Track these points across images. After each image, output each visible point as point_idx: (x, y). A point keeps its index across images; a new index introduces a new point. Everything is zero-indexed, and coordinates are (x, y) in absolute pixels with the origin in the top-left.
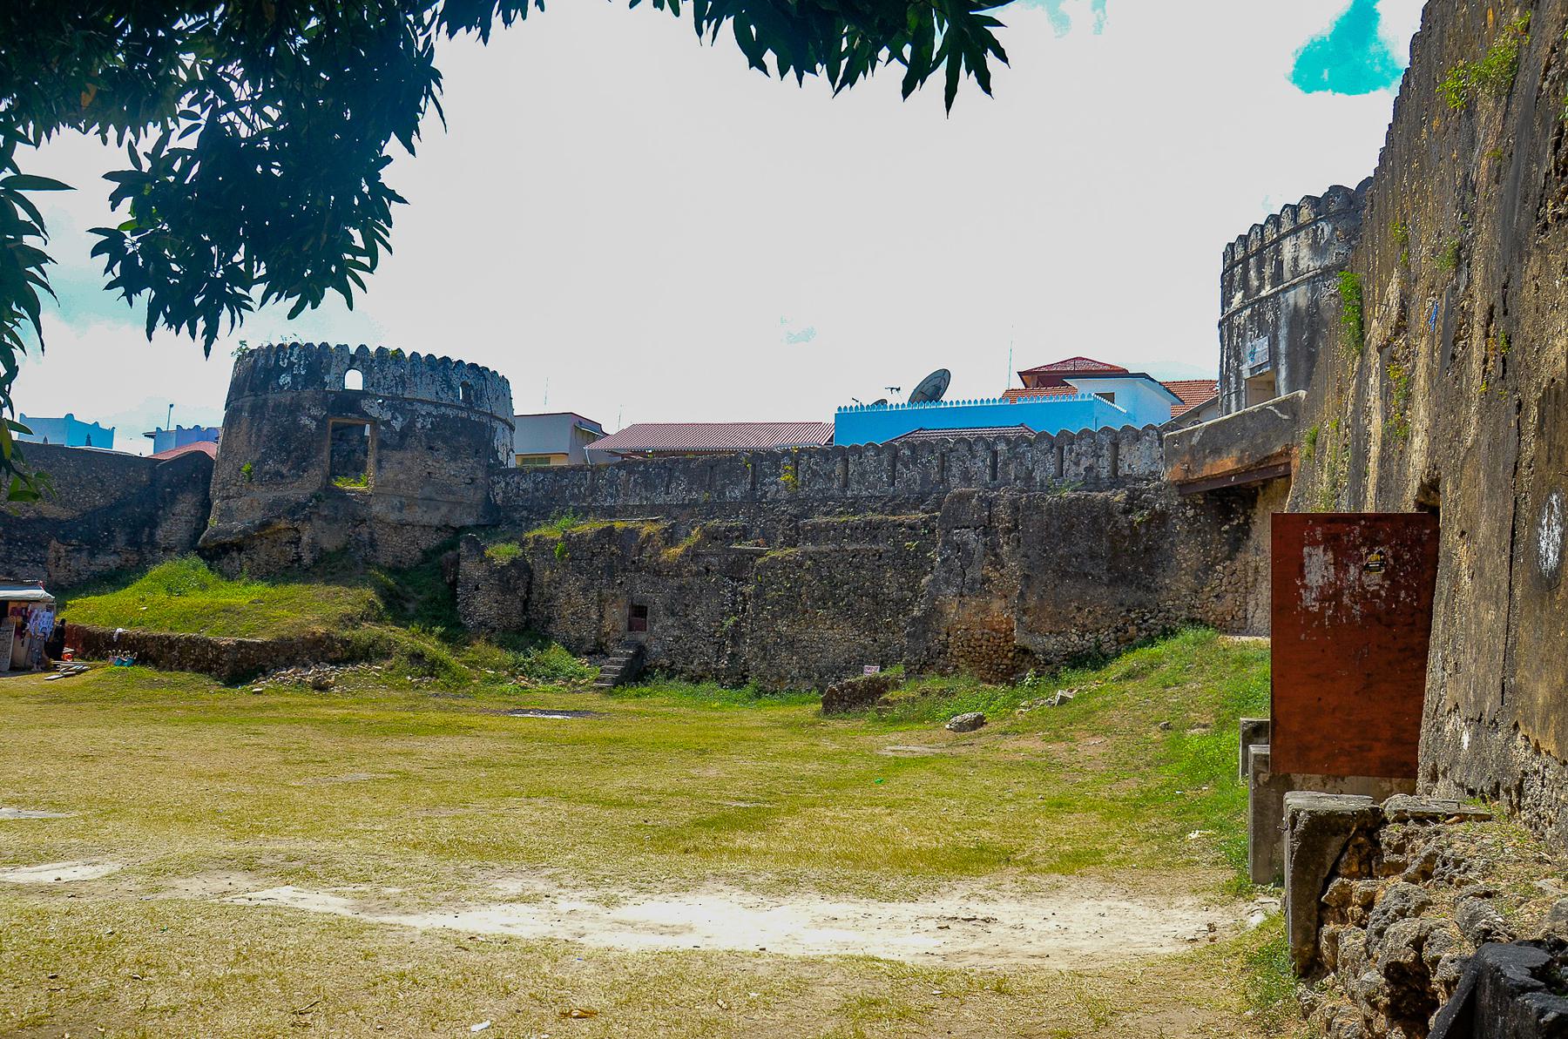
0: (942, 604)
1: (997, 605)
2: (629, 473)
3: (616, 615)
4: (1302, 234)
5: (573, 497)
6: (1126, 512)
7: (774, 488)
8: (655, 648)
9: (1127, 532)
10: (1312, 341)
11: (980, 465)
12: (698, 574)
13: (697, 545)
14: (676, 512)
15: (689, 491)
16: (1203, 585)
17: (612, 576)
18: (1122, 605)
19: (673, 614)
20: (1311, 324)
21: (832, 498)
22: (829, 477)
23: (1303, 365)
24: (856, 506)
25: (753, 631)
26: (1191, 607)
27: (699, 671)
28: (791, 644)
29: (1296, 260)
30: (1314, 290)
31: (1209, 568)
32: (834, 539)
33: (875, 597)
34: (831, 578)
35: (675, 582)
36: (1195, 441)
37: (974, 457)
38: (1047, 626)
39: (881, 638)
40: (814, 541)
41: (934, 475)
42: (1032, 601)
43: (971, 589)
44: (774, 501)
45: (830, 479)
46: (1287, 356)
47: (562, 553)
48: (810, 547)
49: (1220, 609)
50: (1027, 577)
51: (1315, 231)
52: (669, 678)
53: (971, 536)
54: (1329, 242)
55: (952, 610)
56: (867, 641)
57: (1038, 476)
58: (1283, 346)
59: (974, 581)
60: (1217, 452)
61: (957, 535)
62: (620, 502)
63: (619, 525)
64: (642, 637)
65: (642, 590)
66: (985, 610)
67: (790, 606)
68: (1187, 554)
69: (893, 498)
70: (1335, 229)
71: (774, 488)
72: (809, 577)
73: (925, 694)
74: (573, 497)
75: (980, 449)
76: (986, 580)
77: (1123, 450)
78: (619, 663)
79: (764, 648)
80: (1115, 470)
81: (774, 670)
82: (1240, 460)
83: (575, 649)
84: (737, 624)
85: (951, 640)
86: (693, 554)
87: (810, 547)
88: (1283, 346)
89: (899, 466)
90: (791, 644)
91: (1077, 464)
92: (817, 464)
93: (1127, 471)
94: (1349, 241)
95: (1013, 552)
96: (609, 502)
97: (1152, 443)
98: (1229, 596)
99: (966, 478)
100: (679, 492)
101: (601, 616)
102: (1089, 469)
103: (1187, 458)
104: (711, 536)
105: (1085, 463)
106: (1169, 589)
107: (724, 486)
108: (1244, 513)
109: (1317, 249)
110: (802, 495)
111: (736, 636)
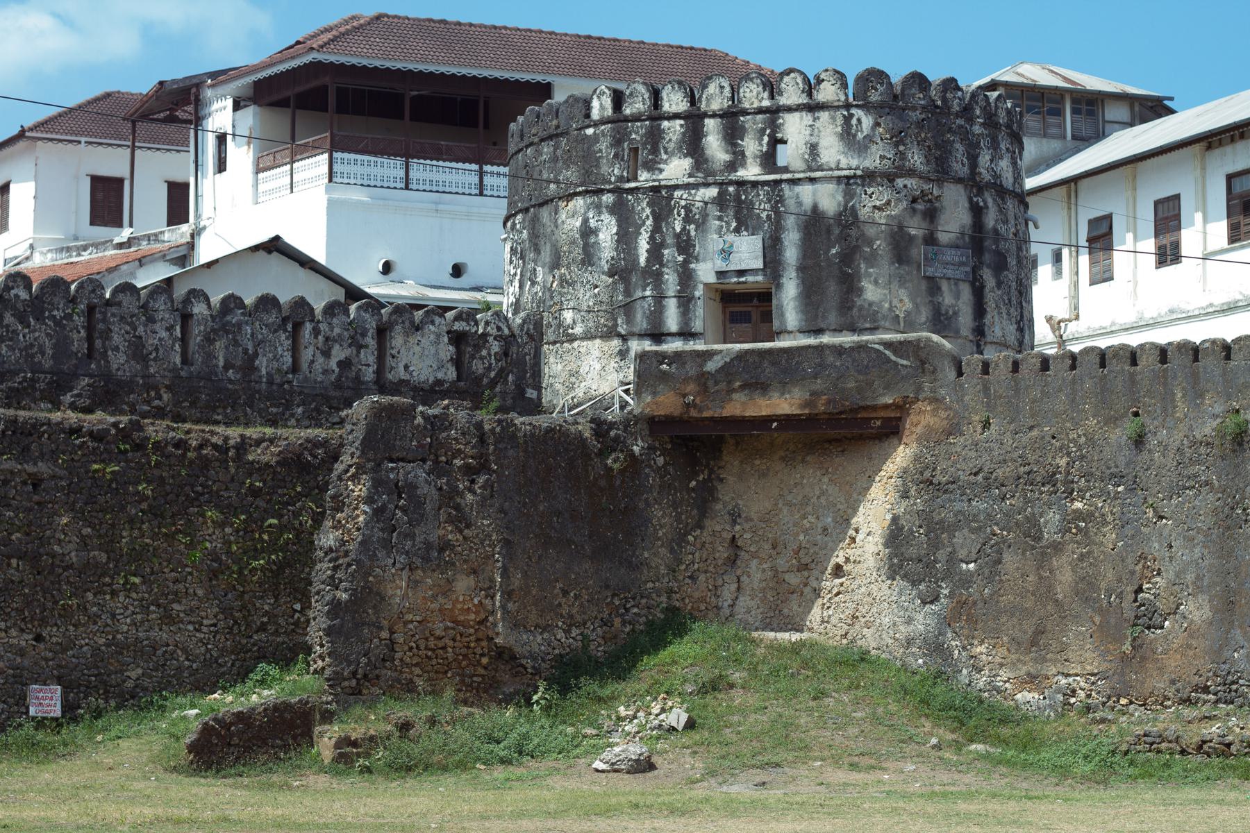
1: (463, 584)
4: (824, 116)
6: (602, 454)
9: (603, 483)
10: (848, 257)
11: (161, 334)
16: (680, 562)
18: (607, 587)
20: (844, 237)
23: (833, 288)
26: (670, 592)
29: (813, 148)
30: (849, 195)
31: (681, 539)
33: (34, 559)
36: (711, 366)
38: (533, 618)
39: (54, 634)
41: (78, 340)
42: (517, 580)
43: (426, 559)
46: (802, 269)
49: (696, 595)
50: (507, 543)
51: (848, 119)
53: (419, 473)
54: (869, 139)
55: (398, 589)
57: (262, 363)
58: (791, 254)
59: (429, 546)
60: (758, 386)
61: (397, 472)
66: (446, 590)
68: (661, 518)
70: (877, 124)
73: (405, 727)
75: (160, 304)
76: (445, 546)
77: (397, 340)
80: (380, 372)
82: (807, 404)
85: (400, 638)
88: (791, 254)
91: (327, 354)
93: (402, 375)
94: (897, 145)
95: (483, 504)
97: (438, 336)
98: (702, 577)
99: (137, 350)
102: (345, 364)
103: (691, 387)
105: (339, 353)
106: (650, 567)
108: (707, 466)
109: (847, 135)
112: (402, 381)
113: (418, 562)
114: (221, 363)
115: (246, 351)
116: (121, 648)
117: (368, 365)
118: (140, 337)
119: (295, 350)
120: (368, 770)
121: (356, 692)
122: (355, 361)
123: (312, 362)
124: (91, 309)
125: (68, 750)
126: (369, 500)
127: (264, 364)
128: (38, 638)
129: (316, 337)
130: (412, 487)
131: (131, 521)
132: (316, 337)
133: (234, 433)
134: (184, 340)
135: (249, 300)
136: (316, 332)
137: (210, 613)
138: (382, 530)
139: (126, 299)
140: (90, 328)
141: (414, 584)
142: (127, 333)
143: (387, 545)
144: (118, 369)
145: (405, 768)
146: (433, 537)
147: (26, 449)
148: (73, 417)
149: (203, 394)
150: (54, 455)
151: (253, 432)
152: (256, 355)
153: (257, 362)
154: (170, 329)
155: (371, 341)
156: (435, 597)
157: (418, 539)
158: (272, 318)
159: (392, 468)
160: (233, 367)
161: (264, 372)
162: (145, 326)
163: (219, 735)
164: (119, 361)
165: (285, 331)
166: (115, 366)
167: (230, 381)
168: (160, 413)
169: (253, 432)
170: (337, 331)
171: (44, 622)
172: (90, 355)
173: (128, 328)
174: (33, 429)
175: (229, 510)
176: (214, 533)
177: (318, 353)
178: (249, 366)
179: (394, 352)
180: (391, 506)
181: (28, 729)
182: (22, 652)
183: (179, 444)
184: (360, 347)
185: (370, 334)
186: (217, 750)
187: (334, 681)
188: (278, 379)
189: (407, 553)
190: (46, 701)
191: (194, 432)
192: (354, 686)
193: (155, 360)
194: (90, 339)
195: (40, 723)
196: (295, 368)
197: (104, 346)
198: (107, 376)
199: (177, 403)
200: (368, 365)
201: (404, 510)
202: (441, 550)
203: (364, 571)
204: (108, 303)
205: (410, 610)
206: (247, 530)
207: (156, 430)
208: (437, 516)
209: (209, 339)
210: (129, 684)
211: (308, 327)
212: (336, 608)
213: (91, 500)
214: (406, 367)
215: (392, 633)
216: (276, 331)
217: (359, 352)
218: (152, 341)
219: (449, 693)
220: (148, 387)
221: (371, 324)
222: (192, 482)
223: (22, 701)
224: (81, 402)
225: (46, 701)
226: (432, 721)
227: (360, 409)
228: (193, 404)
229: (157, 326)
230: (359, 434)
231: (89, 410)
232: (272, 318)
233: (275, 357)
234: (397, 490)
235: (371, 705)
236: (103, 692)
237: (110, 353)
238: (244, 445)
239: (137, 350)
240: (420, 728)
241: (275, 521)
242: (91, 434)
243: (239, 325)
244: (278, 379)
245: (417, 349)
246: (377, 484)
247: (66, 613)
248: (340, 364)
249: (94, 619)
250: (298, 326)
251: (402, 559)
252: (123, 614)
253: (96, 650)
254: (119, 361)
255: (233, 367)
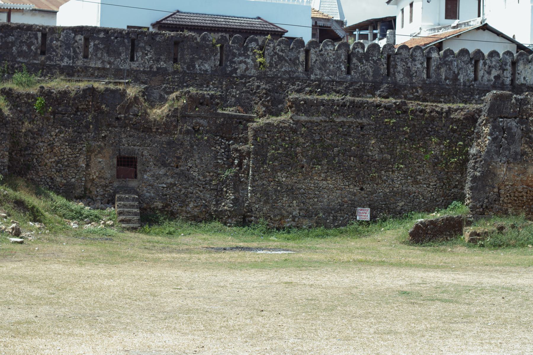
0: (495, 168)
2: (87, 40)
3: (102, 166)
5: (21, 53)
7: (243, 66)
8: (149, 193)
11: (418, 66)
12: (188, 132)
13: (184, 107)
14: (144, 77)
15: (158, 60)
17: (97, 129)
19: (164, 164)
21: (298, 78)
22: (294, 62)
24: (322, 87)
25: (254, 180)
27: (196, 212)
28: (291, 191)
32: (324, 113)
33: (361, 157)
34: (321, 141)
35: (164, 138)
37: (414, 60)
39: (368, 187)
40: (306, 113)
41: (383, 69)
43: (515, 159)
44: (242, 76)
45: (295, 64)
47: (44, 107)
48: (303, 118)
52: (171, 220)
53: (513, 123)
55: (502, 172)
56: (356, 189)
59: (516, 153)
61: (502, 122)
62: (80, 63)
63: (100, 85)
64: (133, 183)
65: (129, 144)
67: (289, 161)
69: (351, 84)
71: (243, 66)
72: (302, 140)
73: (501, 229)
74: (21, 53)
75: (418, 53)
76: (524, 153)
77: (520, 67)
78: (132, 206)
79: (266, 194)
80: (512, 81)
81: (277, 212)
83: (69, 193)
84: (236, 175)
85: (502, 192)
86: (178, 116)
87: (303, 118)
89: (355, 60)
90: (291, 191)
91: (489, 73)
92: (282, 51)
93: (522, 81)
96: (66, 62)
99: (408, 73)
100: (144, 60)
101: (88, 165)
102: (497, 77)
104: (197, 102)
105: (494, 73)
107: (193, 60)
110: (270, 74)
111: (237, 183)
112: (522, 84)
113: (511, 160)
114: (444, 78)
115: (454, 72)
116: (396, 194)
117: (508, 78)
118: (409, 67)
119: (476, 72)
120: (482, 246)
121: (482, 214)
122: (502, 76)
123: (483, 76)
124: (389, 57)
125: (370, 233)
126: (491, 134)
127: (462, 78)
128: (362, 189)
129: (485, 66)
130: (510, 129)
131: (401, 142)
132: (485, 66)
133: (446, 106)
134: (428, 68)
135: (456, 51)
136: (485, 64)
137: (433, 181)
138: (496, 147)
139: (403, 52)
140: (388, 64)
141: (509, 169)
142: (404, 65)
143: (498, 153)
144: (400, 81)
145: (497, 246)
146: (518, 150)
147: (358, 113)
148: (378, 100)
149: (435, 90)
150: (369, 115)
151: (454, 106)
152: (458, 74)
153: (459, 77)
154: (422, 64)
155: (509, 67)
156: (518, 175)
157: (511, 151)
158: (466, 58)
159: (501, 121)
160: (448, 79)
161: (462, 81)
162: (411, 62)
163: (422, 229)
164: (400, 77)
165: (471, 63)
166: (399, 79)
167: (447, 85)
168: (417, 98)
169: (454, 106)
170: (494, 63)
171: (364, 183)
172: (388, 75)
173: (404, 64)
174: (361, 105)
175: (442, 138)
176: (436, 147)
177: (485, 73)
178: (455, 78)
179: (519, 72)
180: (500, 137)
181: (355, 225)
182: (355, 194)
183: (422, 111)
184: (504, 70)
185: (508, 64)
186: (420, 236)
187: (473, 209)
188: (468, 84)
189: (506, 156)
190: (364, 214)
191: (429, 106)
192: (481, 211)
193: (415, 76)
194: (388, 68)
195: (361, 223)
196: (476, 79)
197: (394, 71)
198: (395, 83)
199: (424, 94)
200: (508, 78)
201: (506, 139)
202: (522, 155)
203: (487, 163)
204: (397, 54)
205: (507, 180)
206: (450, 146)
207: (412, 105)
208: (520, 141)
209: (438, 68)
210: (399, 208)
211: (481, 62)
212: (475, 178)
213: (385, 133)
214: (524, 78)
215: (499, 189)
216: (467, 64)
217: (503, 72)
218: (414, 69)
219: (523, 215)
220: (412, 88)
221: (509, 60)
222: (426, 127)
223: (354, 214)
224: (383, 94)
225: (364, 214)
226: (513, 227)
227: (488, 96)
228: (431, 94)
229: (416, 63)
230: (487, 107)
231: (386, 97)
232: (466, 58)
233: (467, 74)
234: (503, 130)
235: (488, 219)
236: (385, 211)
237: (396, 74)
238: (450, 111)
239: (408, 73)
240: (508, 229)
241: (461, 143)
242: (385, 107)
243: (451, 62)
244: (468, 84)
245: (530, 71)
246: (494, 128)
247: (373, 179)
248: (495, 77)
249: (384, 181)
250: (477, 62)
251: (504, 159)
252: (397, 179)
253: (385, 194)
254: (400, 77)
255: (448, 79)
